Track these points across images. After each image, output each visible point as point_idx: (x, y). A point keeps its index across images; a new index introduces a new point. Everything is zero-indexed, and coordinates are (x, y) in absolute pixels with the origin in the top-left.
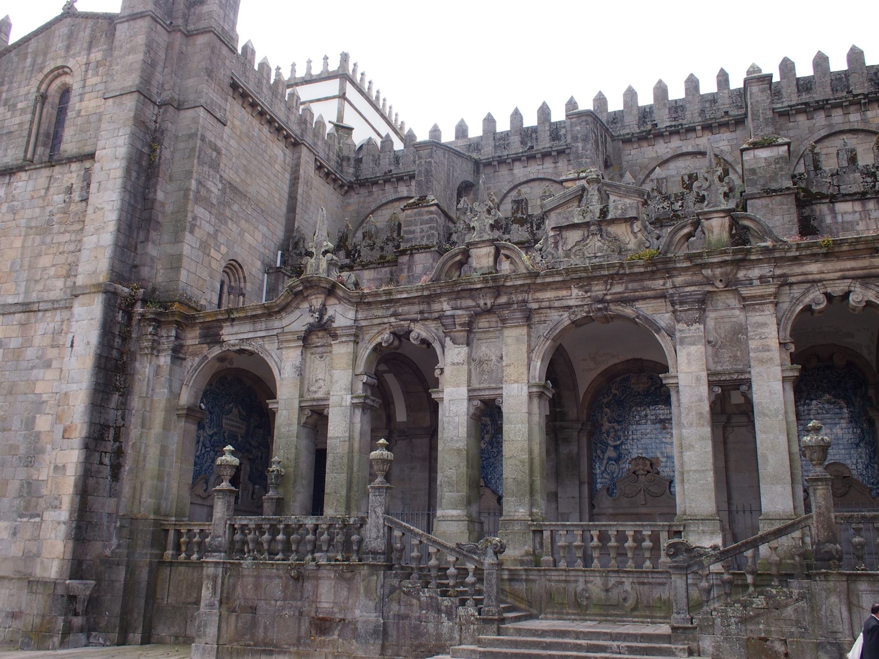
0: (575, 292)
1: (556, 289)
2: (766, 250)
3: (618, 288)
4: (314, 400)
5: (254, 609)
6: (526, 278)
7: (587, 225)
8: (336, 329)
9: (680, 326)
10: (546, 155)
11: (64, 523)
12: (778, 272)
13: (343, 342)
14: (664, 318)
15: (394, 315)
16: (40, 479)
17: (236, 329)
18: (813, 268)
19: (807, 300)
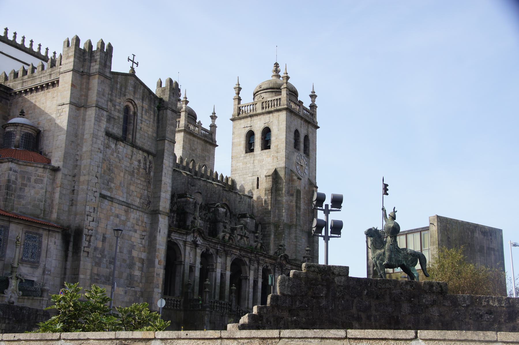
1: (236, 250)
2: (265, 254)
3: (244, 254)
4: (192, 264)
5: (214, 323)
6: (235, 246)
7: (241, 236)
8: (199, 244)
11: (160, 293)
12: (263, 259)
13: (199, 249)
14: (248, 262)
15: (209, 245)
16: (135, 274)
17: (175, 235)
18: (267, 259)
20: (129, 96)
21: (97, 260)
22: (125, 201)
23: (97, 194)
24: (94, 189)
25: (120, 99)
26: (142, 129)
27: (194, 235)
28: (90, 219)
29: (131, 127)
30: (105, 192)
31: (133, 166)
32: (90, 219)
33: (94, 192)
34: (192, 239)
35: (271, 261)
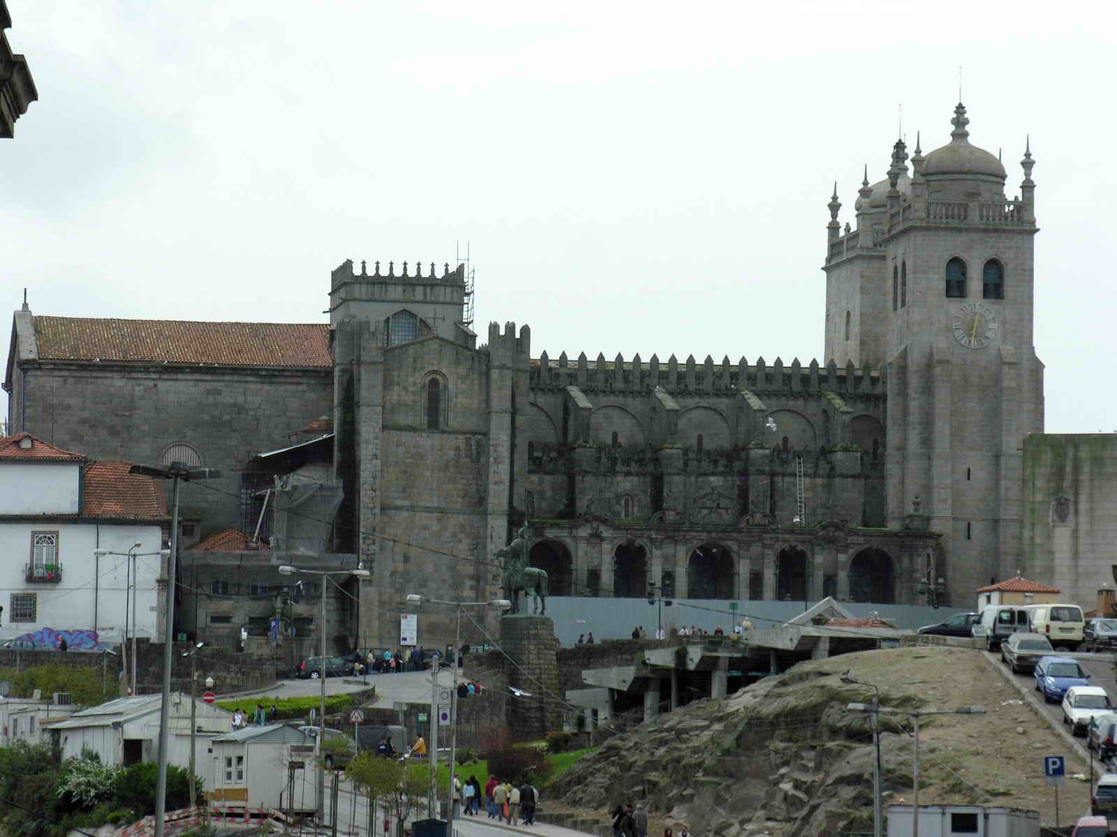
0: (704, 534)
3: (720, 535)
7: (711, 508)
9: (741, 552)
10: (622, 392)
14: (735, 548)
17: (552, 531)
18: (787, 536)
19: (783, 547)
20: (431, 368)
21: (398, 586)
22: (436, 505)
23: (377, 511)
24: (370, 506)
25: (414, 376)
26: (459, 405)
27: (592, 526)
28: (371, 541)
29: (442, 405)
30: (398, 503)
31: (446, 458)
32: (368, 541)
33: (372, 509)
34: (590, 531)
35: (798, 536)
